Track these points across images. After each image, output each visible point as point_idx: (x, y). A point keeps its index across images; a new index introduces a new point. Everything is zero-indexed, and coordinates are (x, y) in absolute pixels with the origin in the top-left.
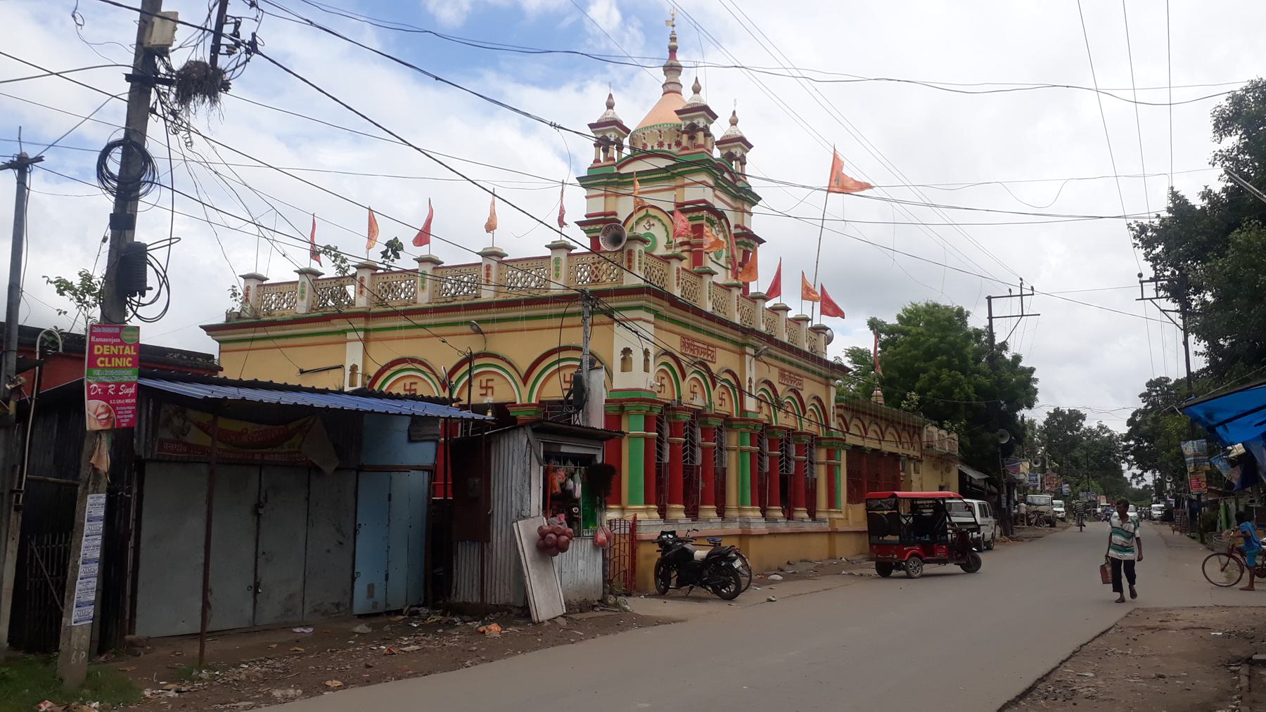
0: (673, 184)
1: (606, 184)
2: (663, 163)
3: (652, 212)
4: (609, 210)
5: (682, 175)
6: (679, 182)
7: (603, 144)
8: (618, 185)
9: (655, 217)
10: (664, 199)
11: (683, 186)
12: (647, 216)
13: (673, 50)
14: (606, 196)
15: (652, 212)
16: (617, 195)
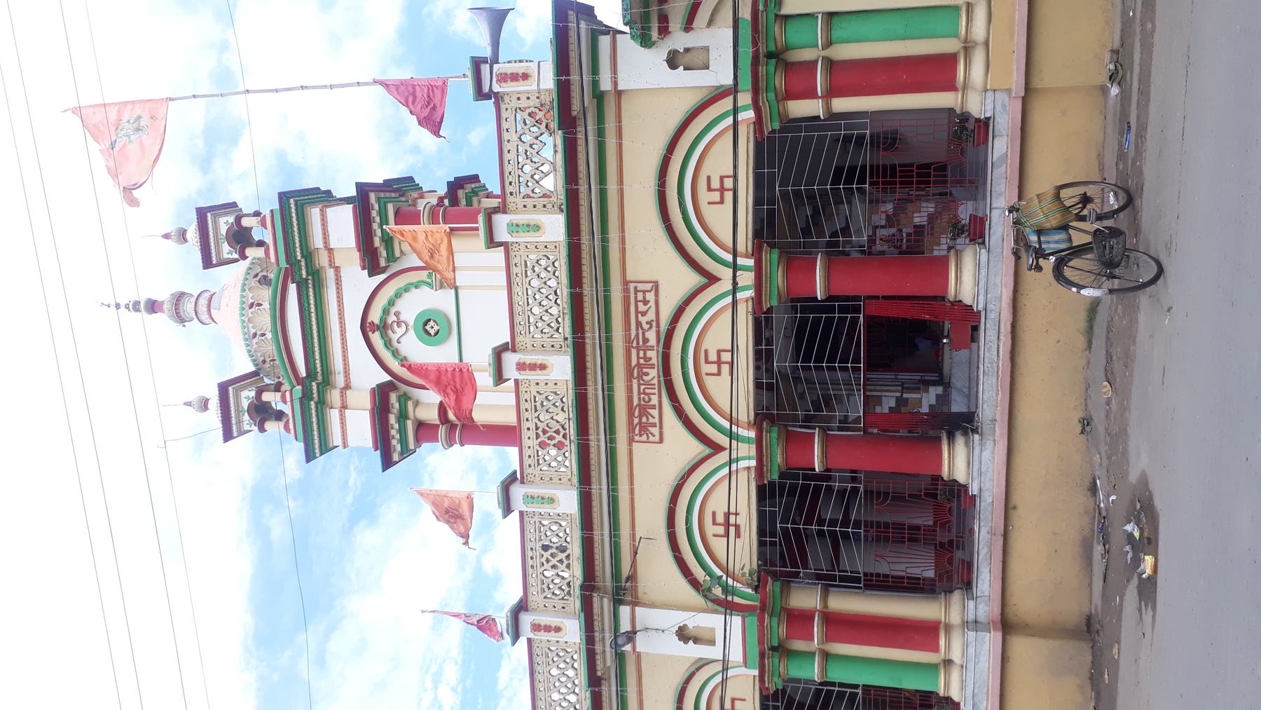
0: (330, 274)
1: (322, 403)
2: (292, 288)
3: (375, 316)
4: (367, 403)
5: (309, 255)
6: (323, 260)
7: (262, 413)
8: (327, 382)
9: (386, 312)
10: (353, 286)
11: (330, 251)
12: (384, 328)
13: (153, 307)
14: (344, 407)
15: (375, 316)
16: (348, 387)
